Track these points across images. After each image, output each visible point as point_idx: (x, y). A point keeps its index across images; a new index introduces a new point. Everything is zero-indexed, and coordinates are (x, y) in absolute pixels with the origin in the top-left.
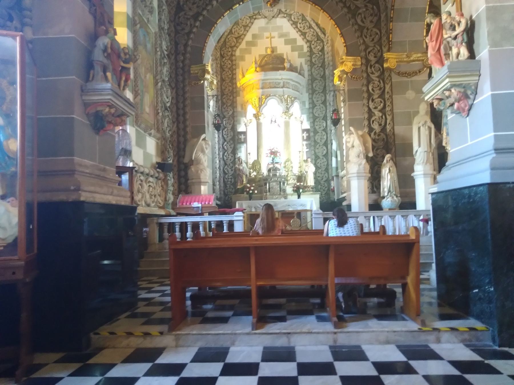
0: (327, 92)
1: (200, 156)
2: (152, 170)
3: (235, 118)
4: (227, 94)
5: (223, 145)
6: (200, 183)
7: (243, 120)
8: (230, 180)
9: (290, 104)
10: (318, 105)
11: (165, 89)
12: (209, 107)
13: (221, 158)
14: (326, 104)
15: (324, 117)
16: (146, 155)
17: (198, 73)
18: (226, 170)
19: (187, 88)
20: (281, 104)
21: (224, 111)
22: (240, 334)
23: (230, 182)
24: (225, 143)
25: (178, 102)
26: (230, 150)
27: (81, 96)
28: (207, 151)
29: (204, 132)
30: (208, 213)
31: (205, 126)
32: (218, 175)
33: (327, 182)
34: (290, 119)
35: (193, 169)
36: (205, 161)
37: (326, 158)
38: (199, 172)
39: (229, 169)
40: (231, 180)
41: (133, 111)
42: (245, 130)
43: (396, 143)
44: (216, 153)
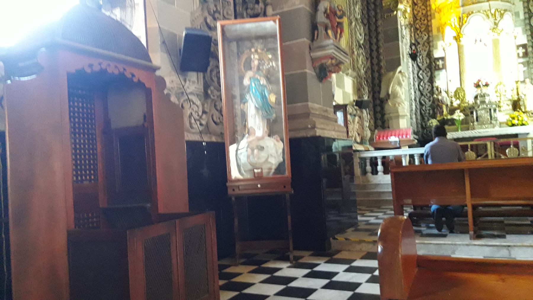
1: (397, 88)
2: (351, 107)
3: (431, 44)
4: (421, 18)
6: (398, 117)
7: (440, 44)
9: (498, 19)
11: (358, 27)
12: (403, 38)
16: (345, 94)
17: (390, 5)
18: (423, 102)
19: (380, 22)
20: (487, 20)
22: (459, 245)
24: (421, 72)
25: (370, 37)
26: (426, 79)
27: (310, 53)
28: (403, 84)
29: (399, 64)
30: (407, 147)
31: (400, 58)
35: (390, 104)
38: (397, 105)
41: (347, 58)
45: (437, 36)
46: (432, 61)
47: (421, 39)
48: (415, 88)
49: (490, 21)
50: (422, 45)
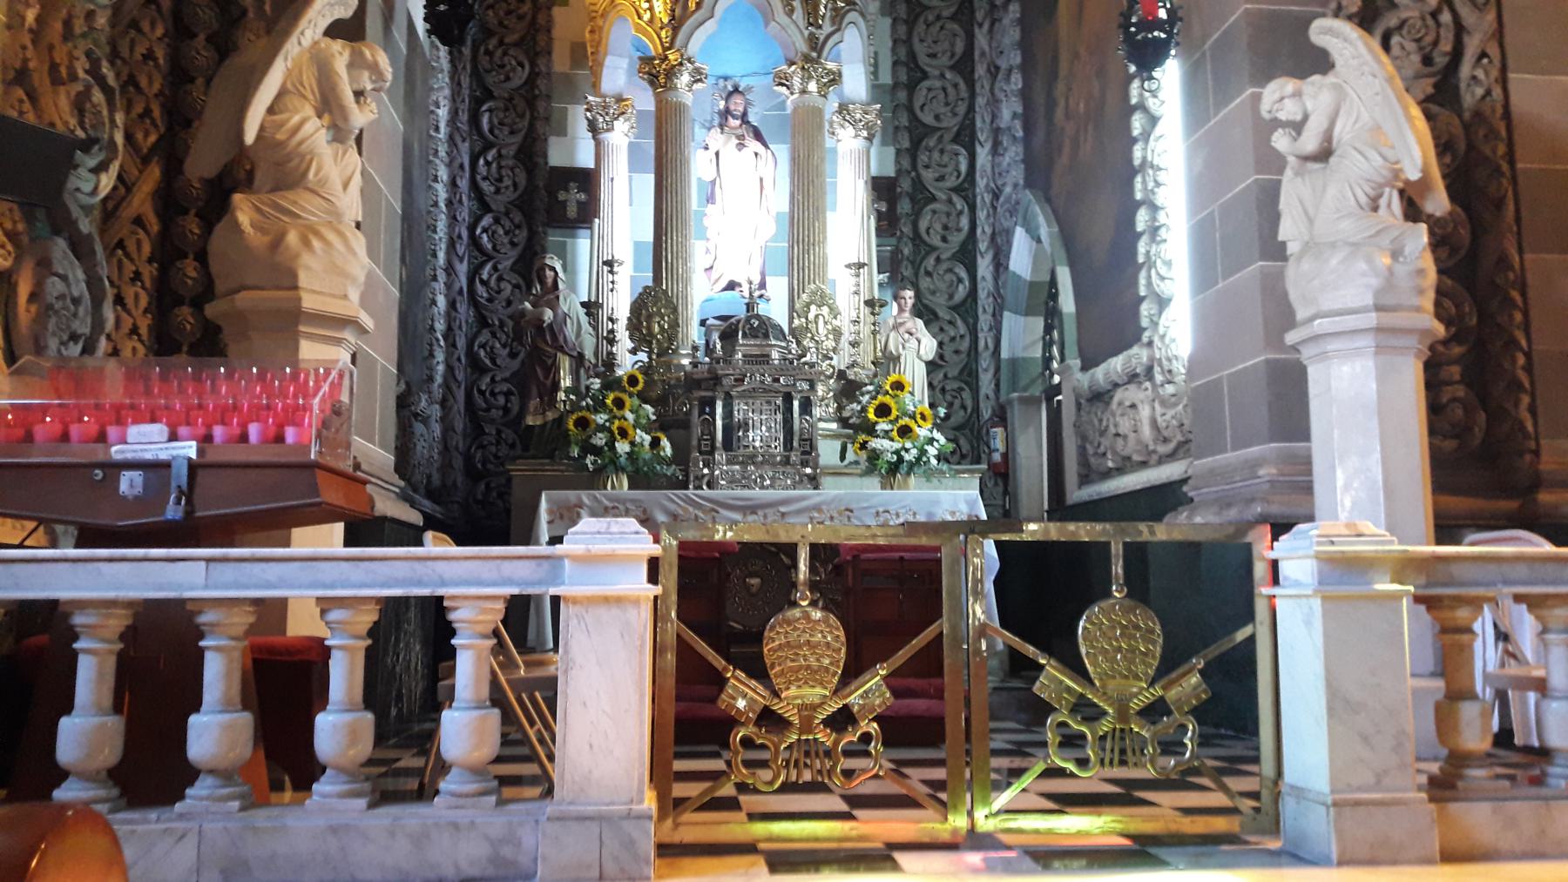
0: (979, 16)
1: (309, 128)
3: (541, 105)
5: (472, 229)
7: (578, 118)
8: (501, 400)
10: (937, 73)
13: (461, 292)
14: (973, 71)
15: (958, 134)
18: (482, 353)
20: (784, 19)
21: (488, 66)
23: (501, 413)
24: (487, 220)
28: (360, 117)
32: (441, 368)
33: (967, 431)
36: (346, 186)
37: (965, 321)
38: (292, 238)
40: (507, 401)
42: (592, 166)
43: (1520, 166)
44: (435, 255)
45: (569, 80)
47: (502, 77)
48: (457, 287)
49: (795, 23)
50: (501, 104)
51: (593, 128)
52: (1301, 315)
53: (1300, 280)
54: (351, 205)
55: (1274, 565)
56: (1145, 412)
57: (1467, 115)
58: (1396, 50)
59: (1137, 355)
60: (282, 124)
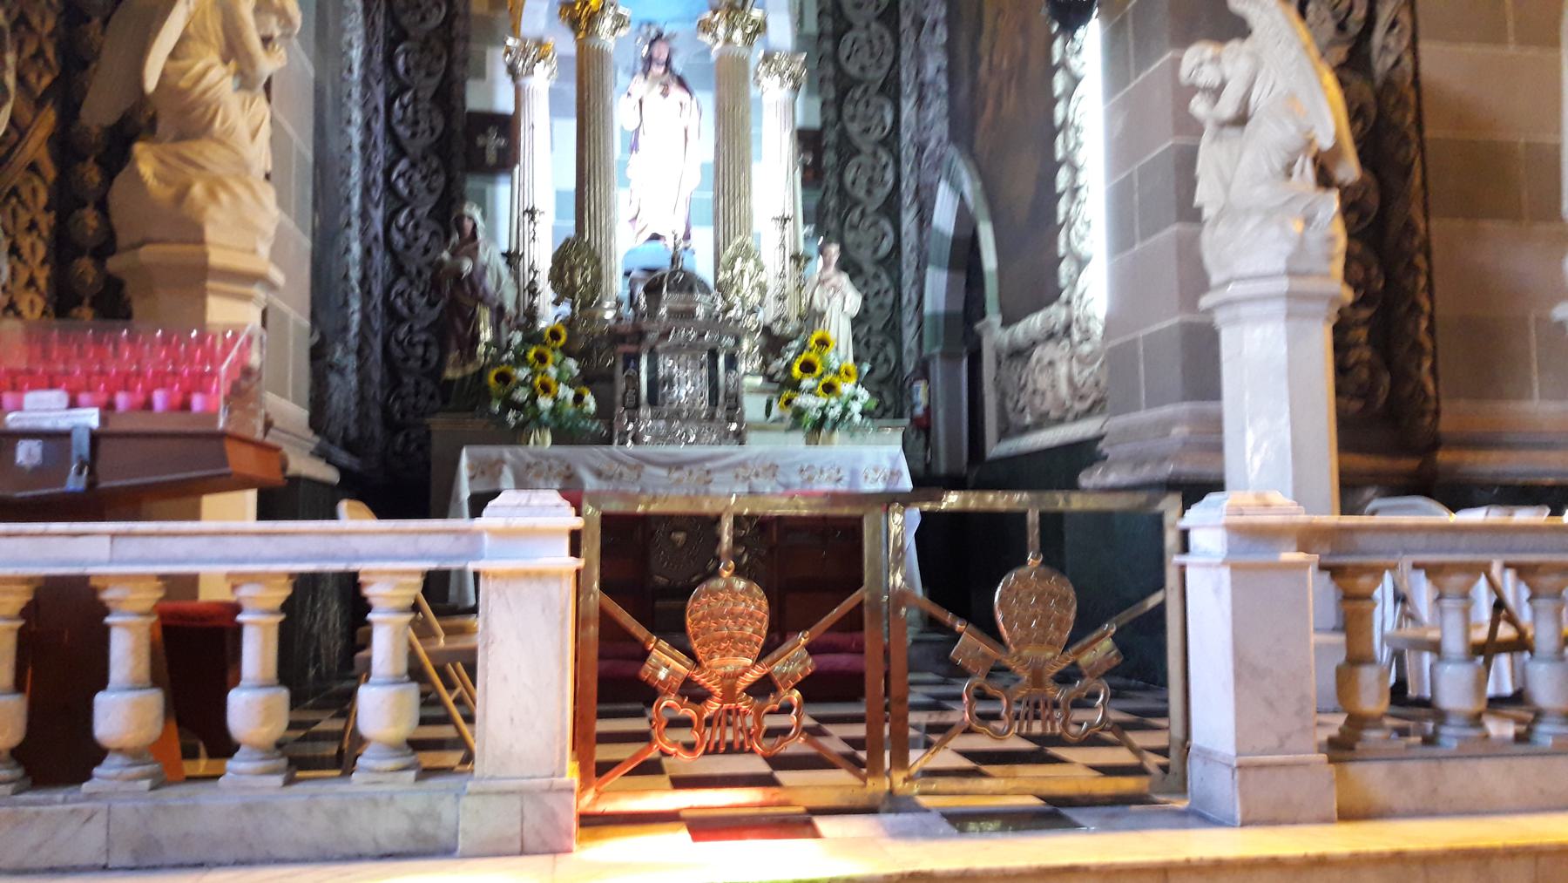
3: (459, 48)
5: (387, 173)
8: (420, 350)
10: (862, 23)
13: (376, 238)
14: (898, 23)
18: (399, 302)
23: (419, 363)
24: (403, 165)
28: (268, 64)
32: (356, 317)
34: (751, 44)
36: (254, 135)
37: (889, 273)
38: (198, 190)
39: (415, 294)
40: (425, 352)
43: (1429, 133)
44: (348, 200)
46: (458, 126)
47: (418, 18)
48: (371, 233)
50: (417, 46)
51: (512, 70)
52: (1215, 278)
53: (1215, 245)
54: (259, 155)
55: (1185, 534)
56: (1062, 370)
57: (1379, 82)
58: (1311, 16)
59: (1055, 314)
60: (184, 72)
